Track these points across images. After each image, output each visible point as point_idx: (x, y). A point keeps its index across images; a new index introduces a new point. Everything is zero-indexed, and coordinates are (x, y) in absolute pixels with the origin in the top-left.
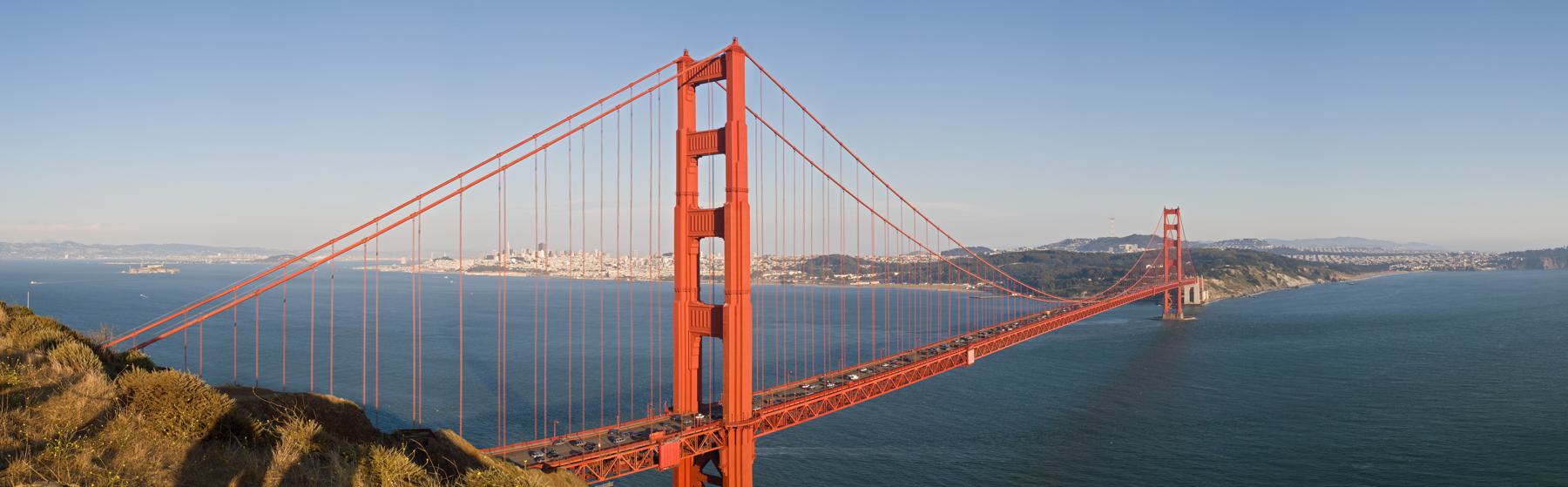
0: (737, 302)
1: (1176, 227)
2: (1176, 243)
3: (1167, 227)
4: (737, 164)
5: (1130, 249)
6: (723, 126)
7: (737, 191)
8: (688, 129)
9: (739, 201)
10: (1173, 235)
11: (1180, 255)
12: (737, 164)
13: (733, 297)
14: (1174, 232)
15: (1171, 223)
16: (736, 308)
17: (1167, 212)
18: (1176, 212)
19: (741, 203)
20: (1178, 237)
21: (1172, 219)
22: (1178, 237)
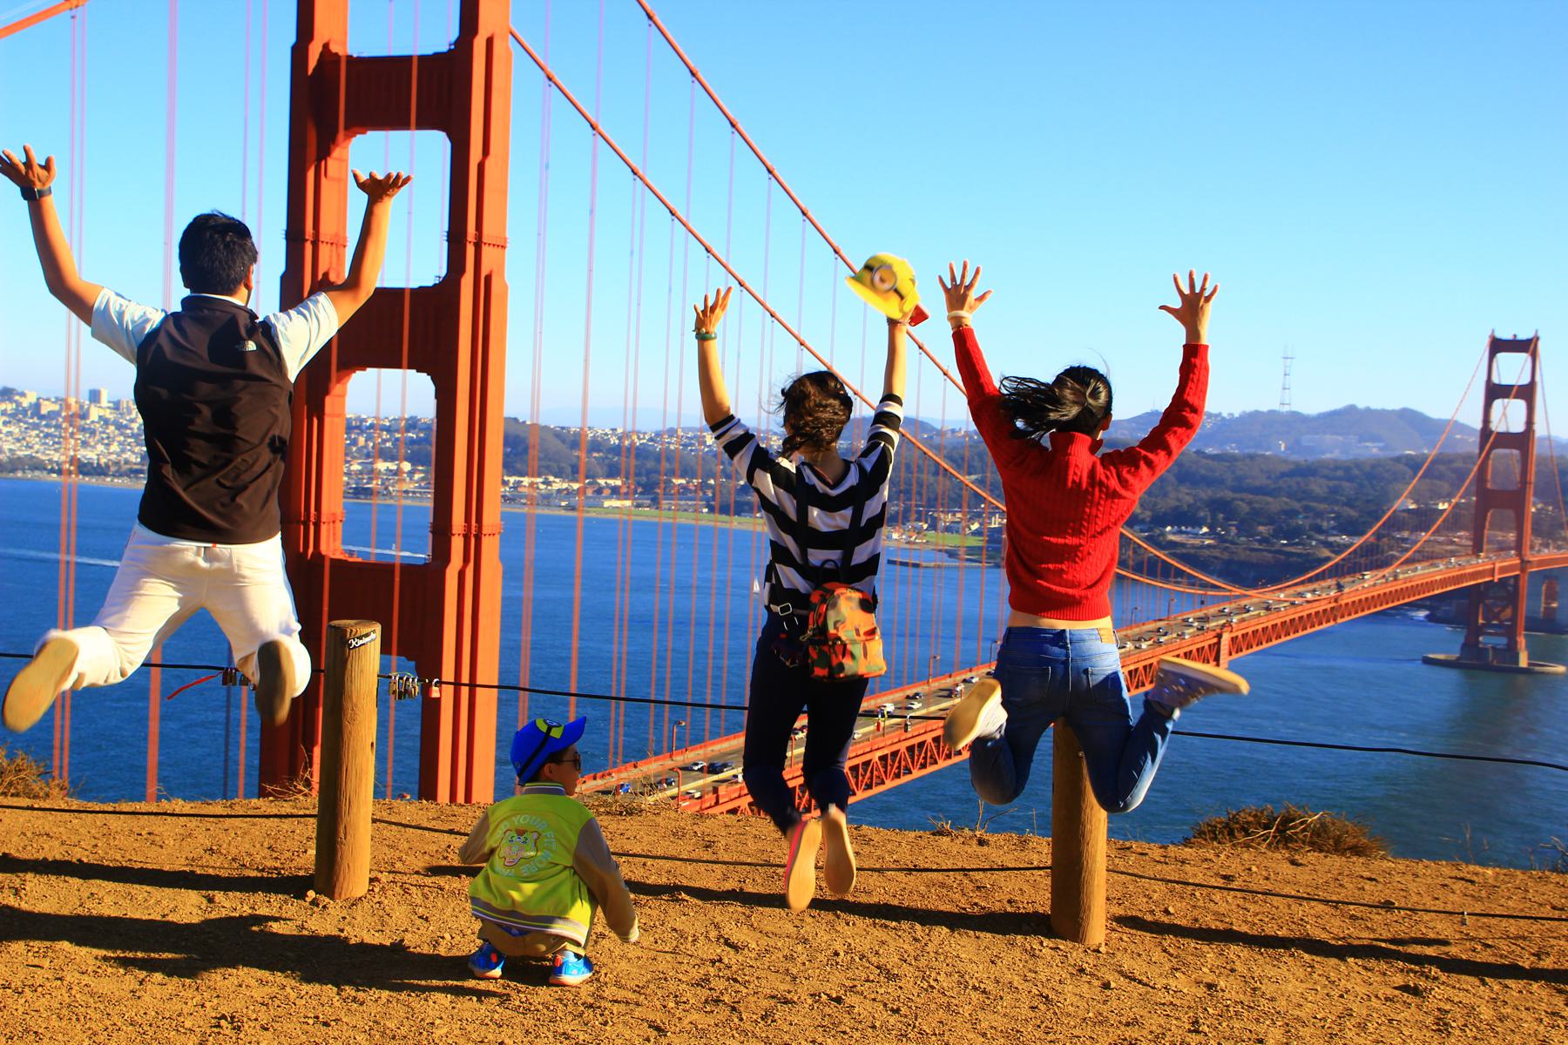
0: (466, 560)
1: (1526, 392)
2: (1522, 441)
3: (1495, 392)
4: (481, 167)
5: (1333, 449)
6: (444, 48)
7: (478, 246)
8: (326, 46)
9: (484, 273)
10: (1510, 417)
11: (1532, 478)
12: (481, 167)
13: (457, 544)
14: (1517, 407)
15: (1504, 382)
16: (462, 575)
17: (1498, 346)
18: (1526, 346)
19: (488, 278)
20: (1530, 422)
21: (1511, 368)
22: (1530, 422)
